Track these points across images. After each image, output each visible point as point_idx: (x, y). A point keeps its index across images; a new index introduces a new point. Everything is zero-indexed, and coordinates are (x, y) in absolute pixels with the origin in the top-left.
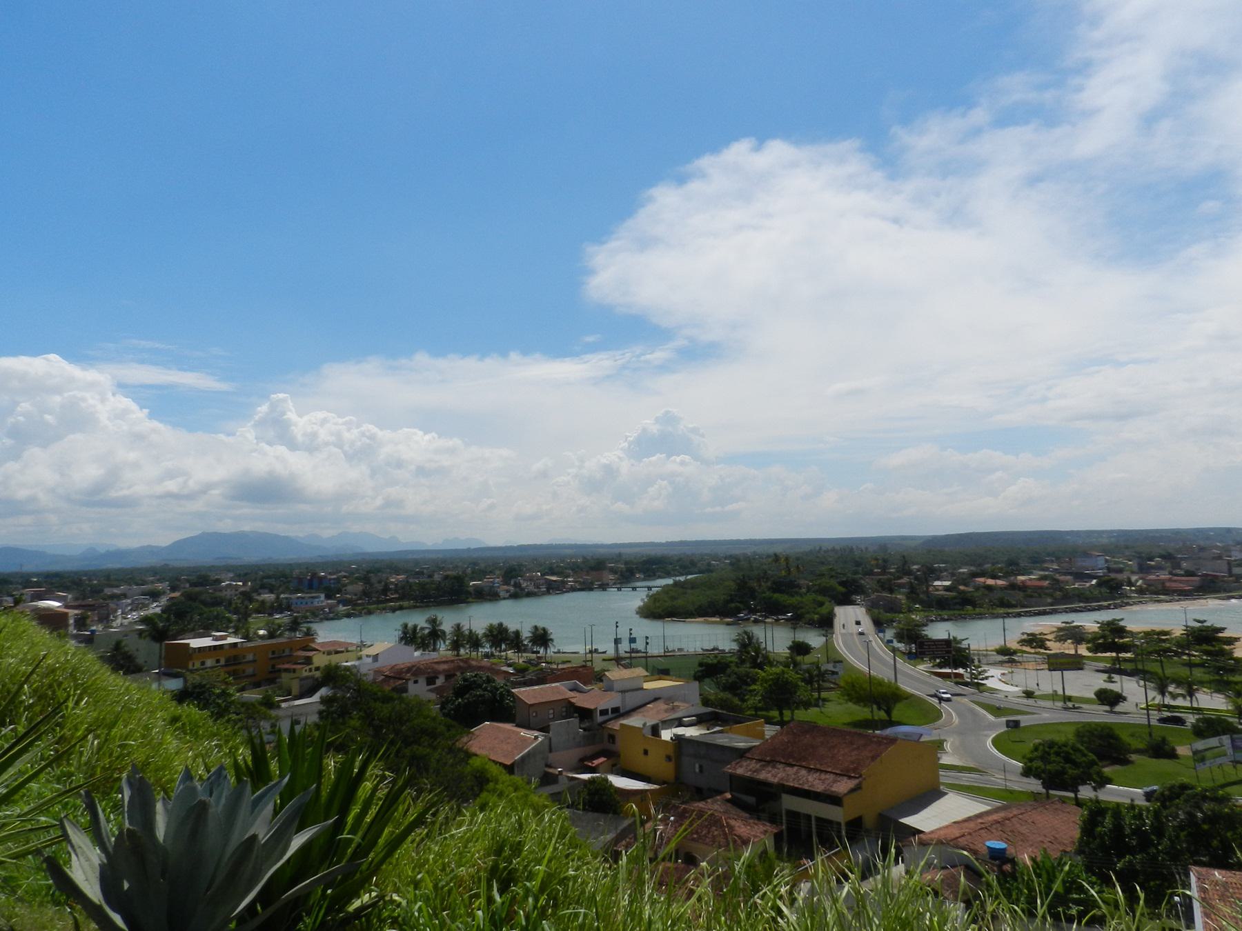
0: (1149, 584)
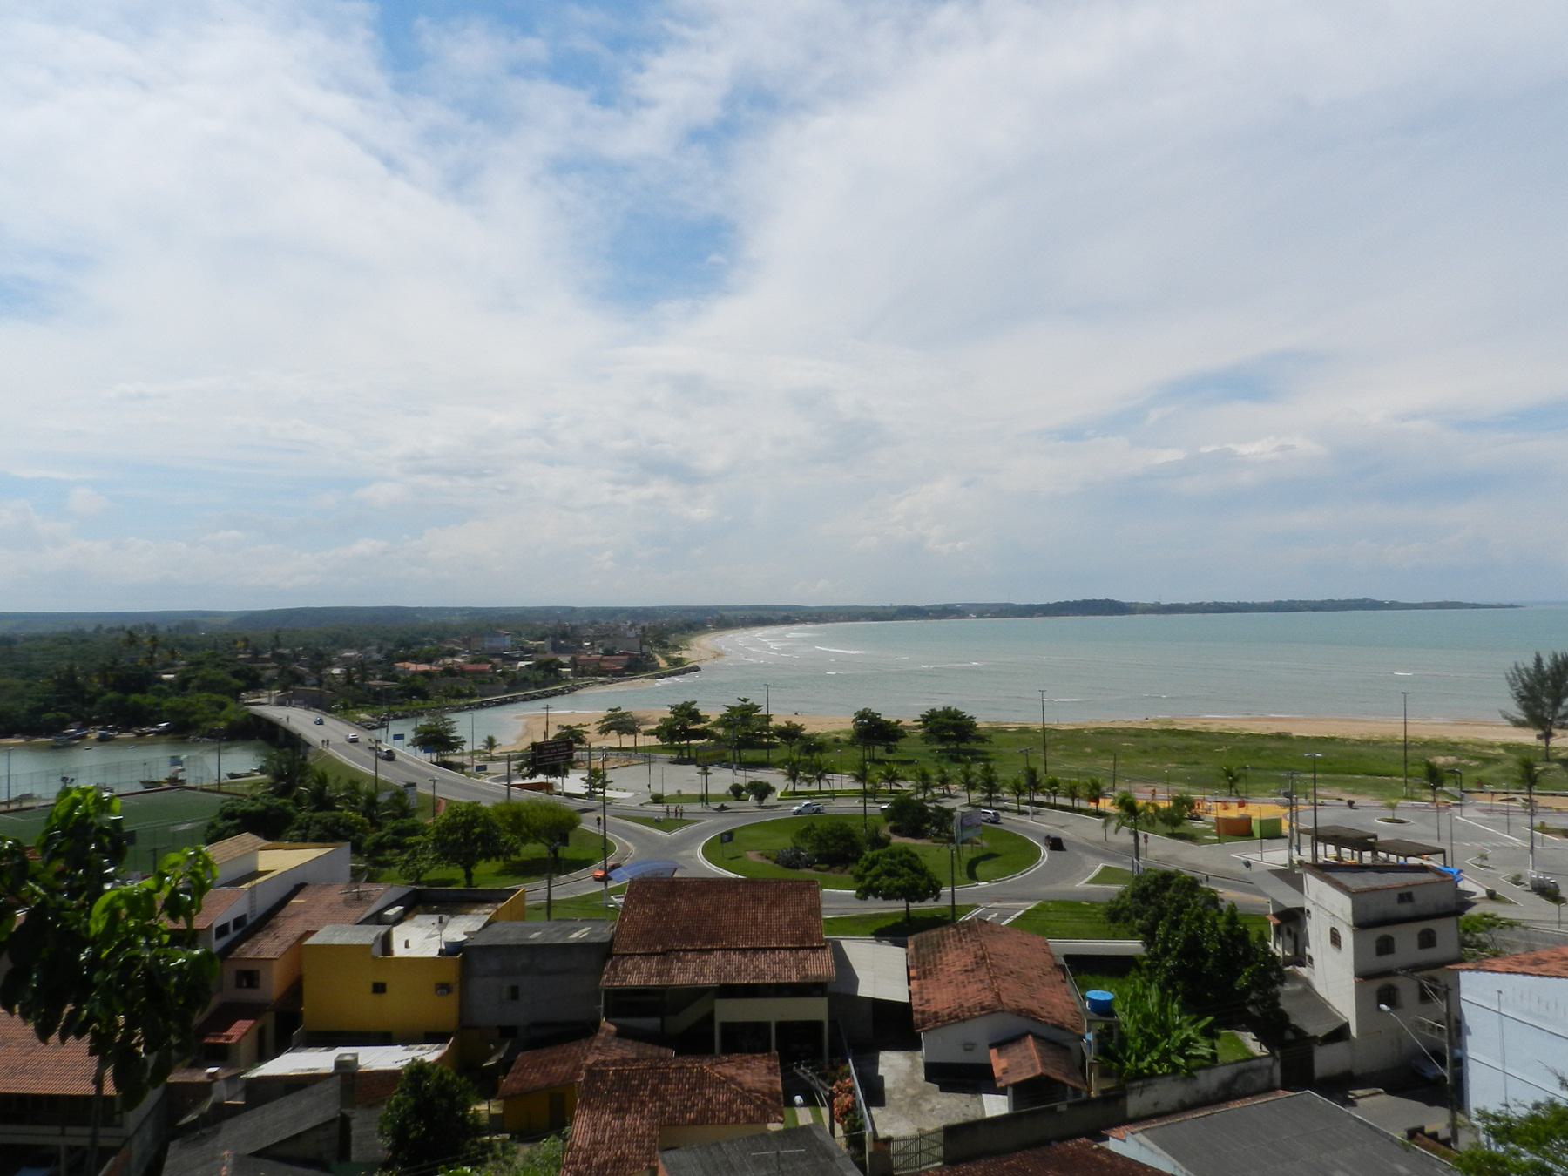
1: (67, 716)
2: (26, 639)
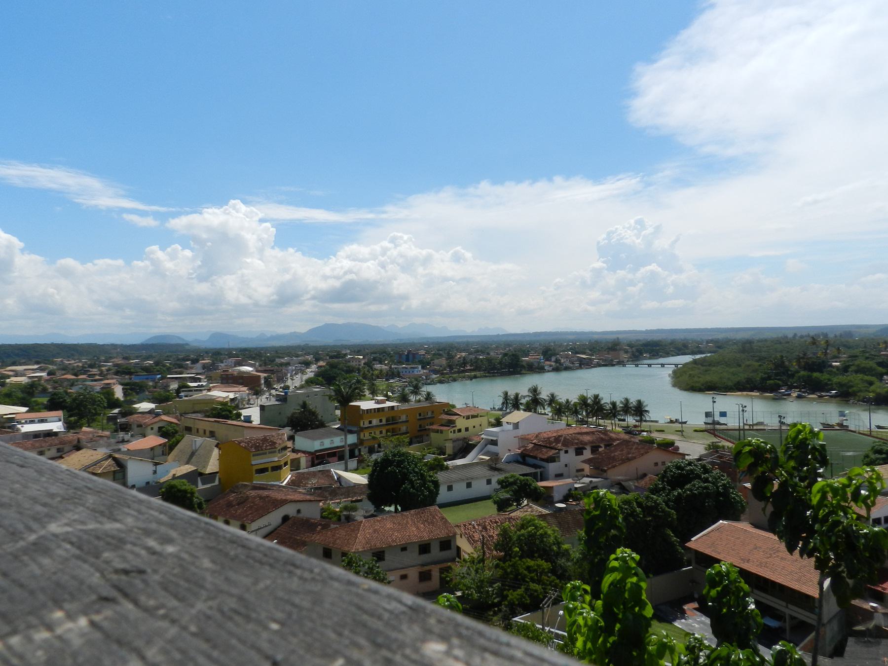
1: (780, 383)
2: (759, 341)
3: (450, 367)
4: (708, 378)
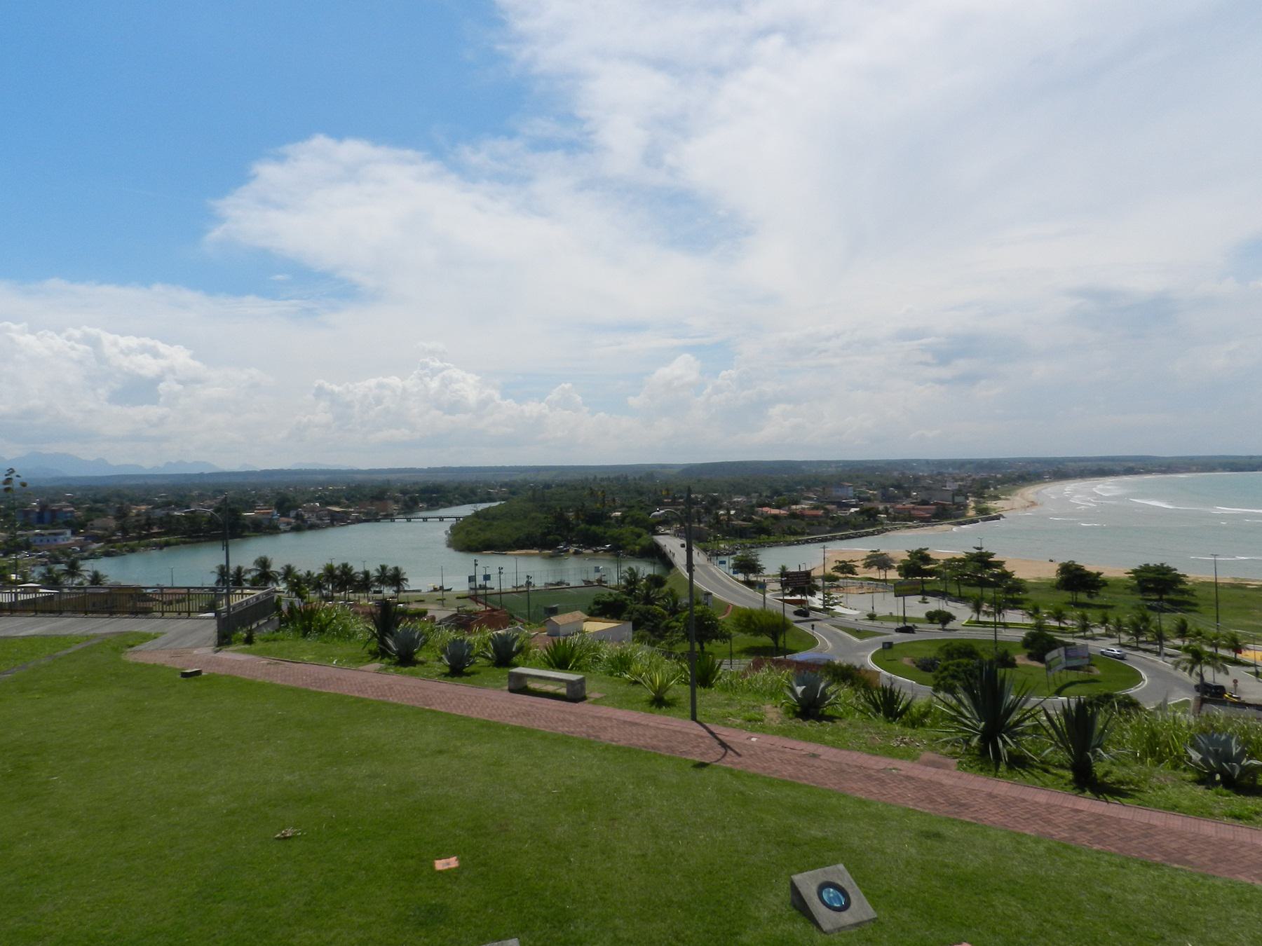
0: (899, 511)
3: (124, 530)
4: (488, 535)
